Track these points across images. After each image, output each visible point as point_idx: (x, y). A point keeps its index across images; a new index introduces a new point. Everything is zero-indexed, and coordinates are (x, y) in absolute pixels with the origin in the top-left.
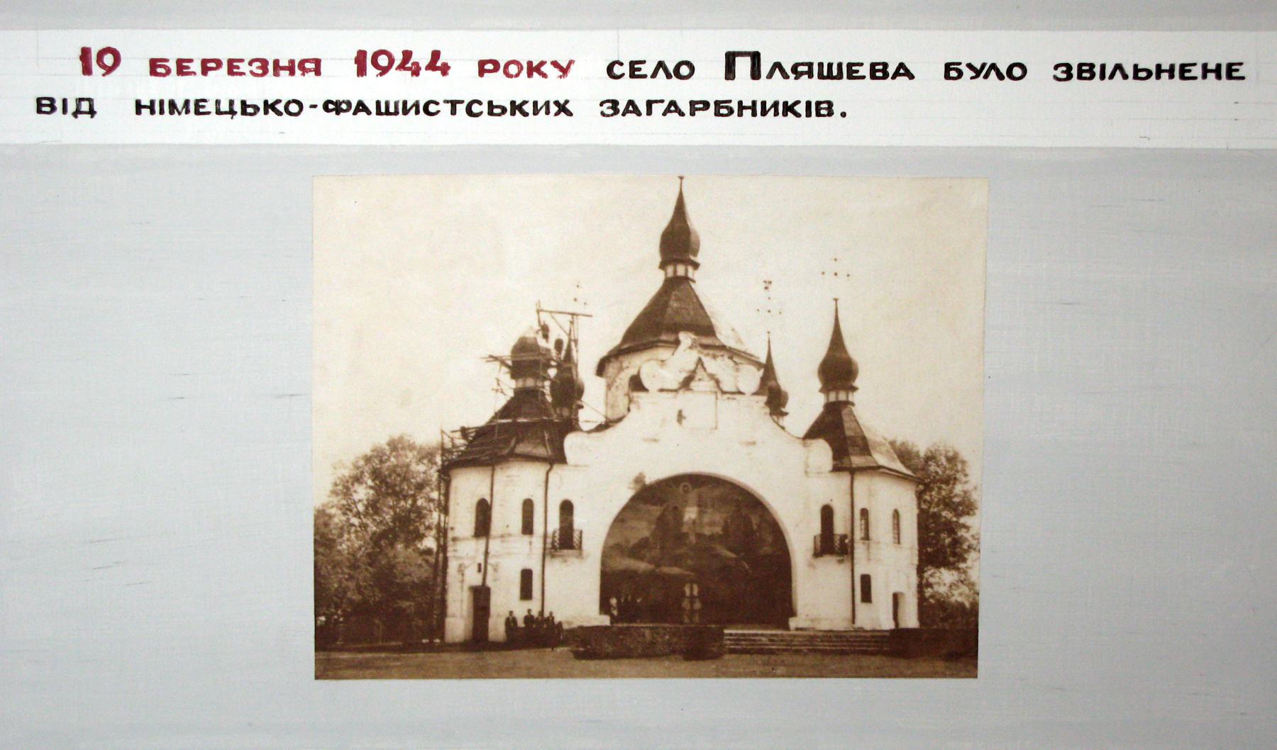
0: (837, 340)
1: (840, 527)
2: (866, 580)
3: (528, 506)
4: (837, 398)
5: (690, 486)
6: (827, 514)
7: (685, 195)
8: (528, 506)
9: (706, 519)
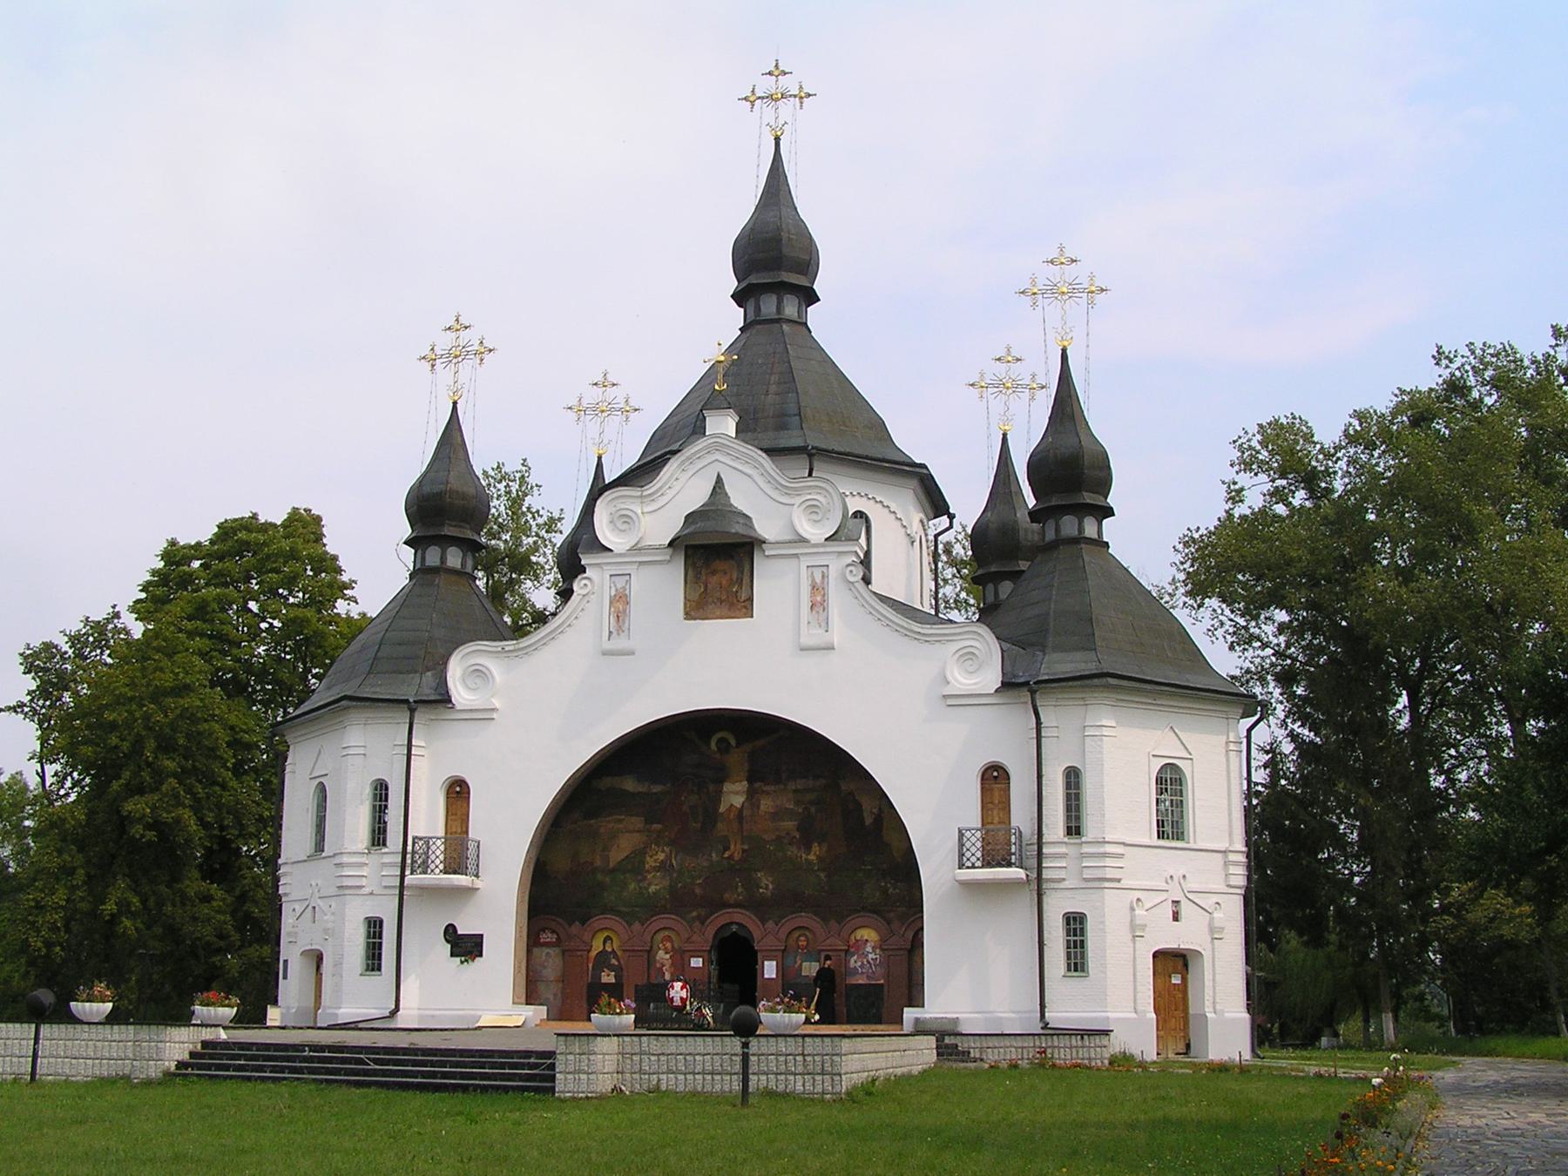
0: (1066, 407)
1: (1021, 816)
2: (1075, 924)
3: (381, 791)
4: (1057, 530)
5: (733, 742)
6: (994, 778)
9: (766, 804)
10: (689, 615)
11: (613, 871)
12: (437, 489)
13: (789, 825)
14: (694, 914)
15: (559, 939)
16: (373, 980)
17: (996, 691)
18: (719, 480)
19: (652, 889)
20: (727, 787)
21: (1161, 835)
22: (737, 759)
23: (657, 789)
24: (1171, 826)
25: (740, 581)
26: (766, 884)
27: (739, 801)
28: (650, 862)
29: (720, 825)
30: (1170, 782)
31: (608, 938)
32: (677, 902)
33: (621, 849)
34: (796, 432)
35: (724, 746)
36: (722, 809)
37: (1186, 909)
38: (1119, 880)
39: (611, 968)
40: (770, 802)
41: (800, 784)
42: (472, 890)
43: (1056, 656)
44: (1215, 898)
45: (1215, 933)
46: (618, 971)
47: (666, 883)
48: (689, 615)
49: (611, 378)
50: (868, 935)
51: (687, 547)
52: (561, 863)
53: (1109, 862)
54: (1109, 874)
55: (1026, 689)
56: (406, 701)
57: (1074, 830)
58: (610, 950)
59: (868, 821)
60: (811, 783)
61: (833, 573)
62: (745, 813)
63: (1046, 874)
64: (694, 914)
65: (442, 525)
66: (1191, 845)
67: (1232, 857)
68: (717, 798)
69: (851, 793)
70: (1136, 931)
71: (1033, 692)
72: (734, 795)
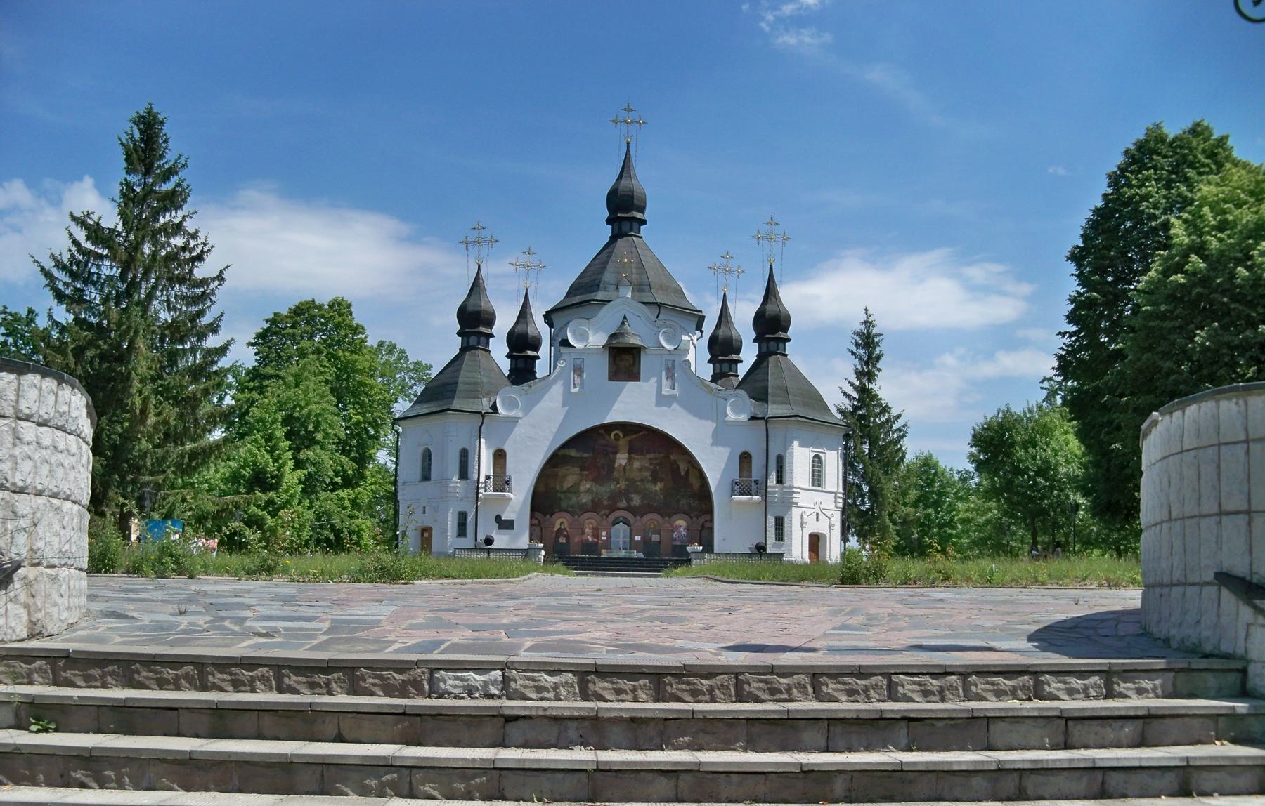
2: (780, 523)
3: (464, 455)
5: (621, 435)
6: (745, 458)
7: (633, 157)
8: (464, 455)
9: (636, 465)
10: (610, 379)
11: (565, 492)
12: (477, 309)
13: (647, 474)
14: (603, 512)
15: (539, 522)
16: (462, 539)
17: (749, 420)
18: (625, 318)
19: (584, 501)
20: (619, 456)
21: (813, 485)
22: (623, 442)
23: (585, 455)
24: (817, 478)
25: (634, 364)
26: (636, 500)
27: (623, 462)
28: (582, 488)
29: (615, 473)
30: (817, 462)
31: (562, 523)
32: (595, 507)
33: (570, 481)
34: (650, 294)
35: (617, 438)
36: (616, 465)
37: (821, 515)
38: (797, 503)
39: (564, 536)
40: (638, 463)
41: (652, 456)
42: (510, 499)
43: (774, 406)
44: (832, 512)
45: (831, 527)
46: (567, 537)
47: (590, 498)
48: (610, 379)
49: (532, 250)
50: (681, 523)
51: (610, 348)
52: (542, 489)
53: (795, 495)
54: (795, 500)
55: (763, 421)
56: (480, 413)
57: (780, 480)
58: (563, 527)
59: (683, 473)
60: (657, 455)
61: (676, 363)
62: (628, 468)
63: (768, 500)
64: (603, 512)
65: (479, 326)
66: (823, 489)
67: (839, 495)
68: (614, 461)
69: (675, 461)
70: (802, 527)
71: (767, 423)
72: (622, 459)
